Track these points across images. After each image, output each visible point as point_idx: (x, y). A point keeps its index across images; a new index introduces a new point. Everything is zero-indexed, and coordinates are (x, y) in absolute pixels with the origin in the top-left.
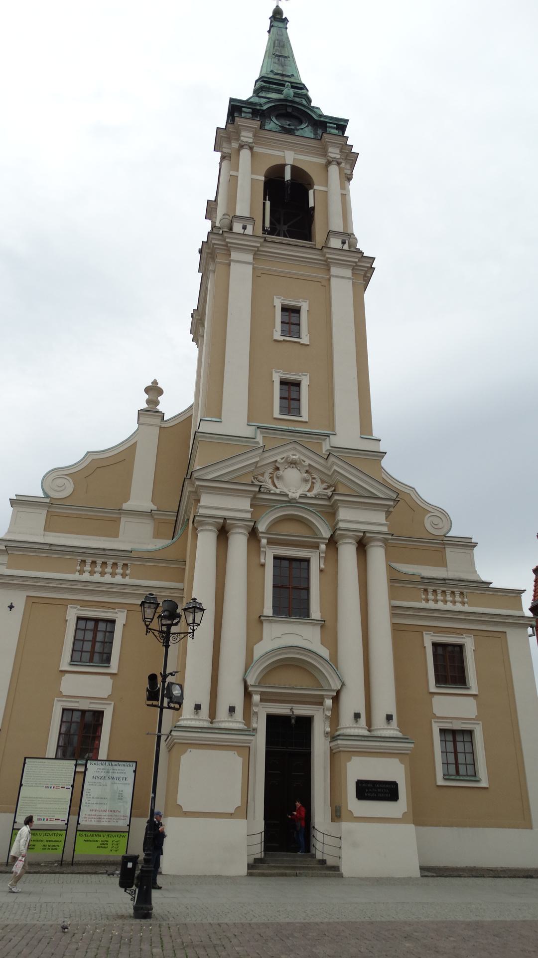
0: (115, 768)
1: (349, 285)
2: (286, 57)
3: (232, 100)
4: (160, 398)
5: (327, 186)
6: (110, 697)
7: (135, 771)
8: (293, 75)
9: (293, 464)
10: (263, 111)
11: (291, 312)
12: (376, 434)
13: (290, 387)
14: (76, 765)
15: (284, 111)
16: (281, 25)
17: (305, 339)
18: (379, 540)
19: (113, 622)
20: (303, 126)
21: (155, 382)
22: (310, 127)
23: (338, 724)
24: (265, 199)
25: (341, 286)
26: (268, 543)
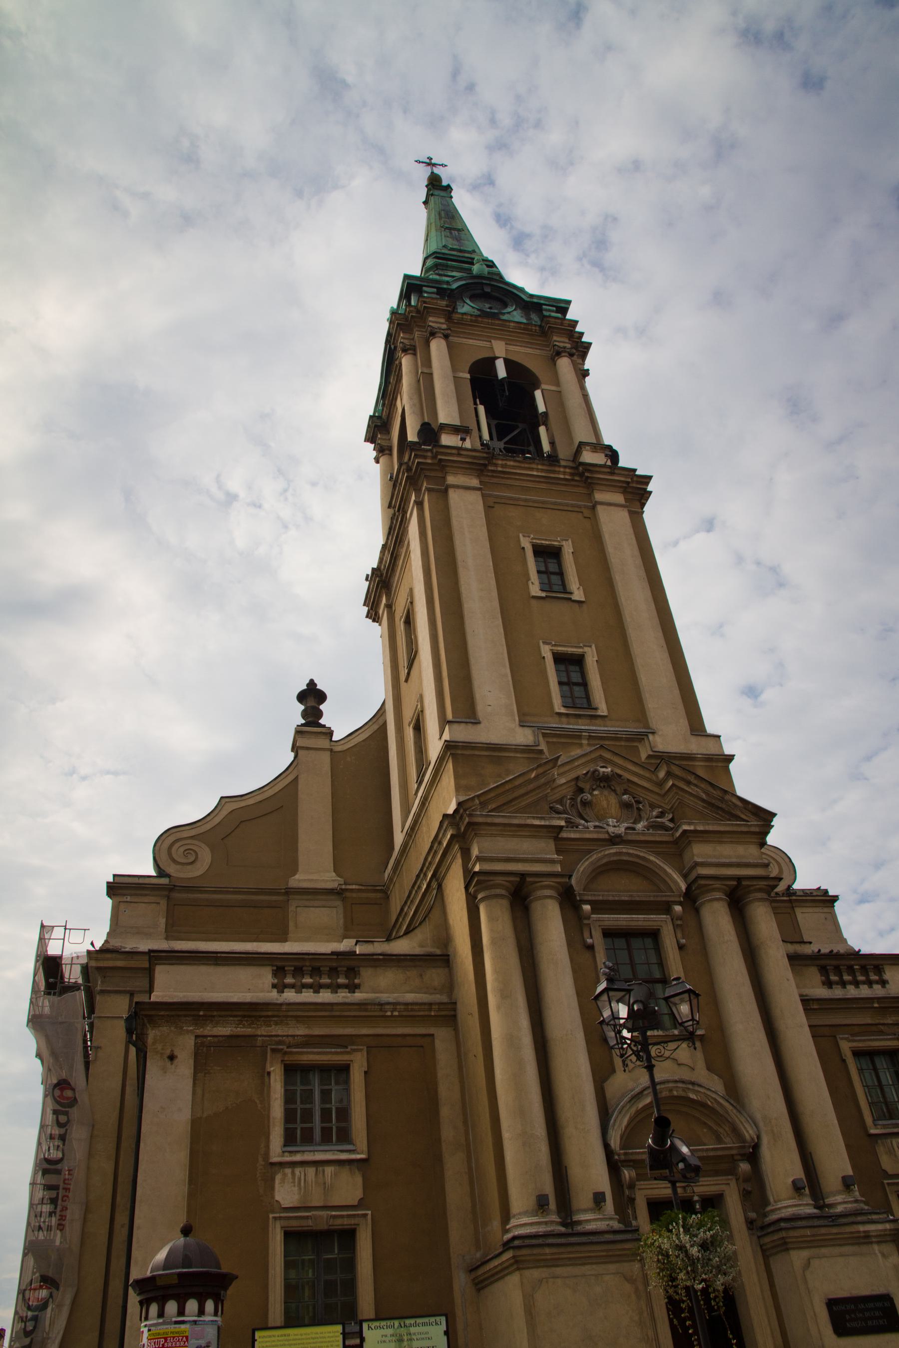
0: (413, 1330)
1: (623, 516)
2: (459, 230)
3: (406, 277)
5: (557, 383)
6: (361, 1204)
7: (446, 1333)
8: (474, 251)
9: (605, 782)
10: (452, 290)
11: (548, 555)
12: (711, 727)
13: (570, 663)
14: (345, 1335)
15: (479, 291)
16: (442, 193)
17: (578, 595)
18: (760, 890)
19: (344, 1069)
20: (509, 309)
21: (312, 684)
22: (519, 311)
23: (765, 1202)
24: (475, 404)
25: (613, 521)
26: (594, 910)
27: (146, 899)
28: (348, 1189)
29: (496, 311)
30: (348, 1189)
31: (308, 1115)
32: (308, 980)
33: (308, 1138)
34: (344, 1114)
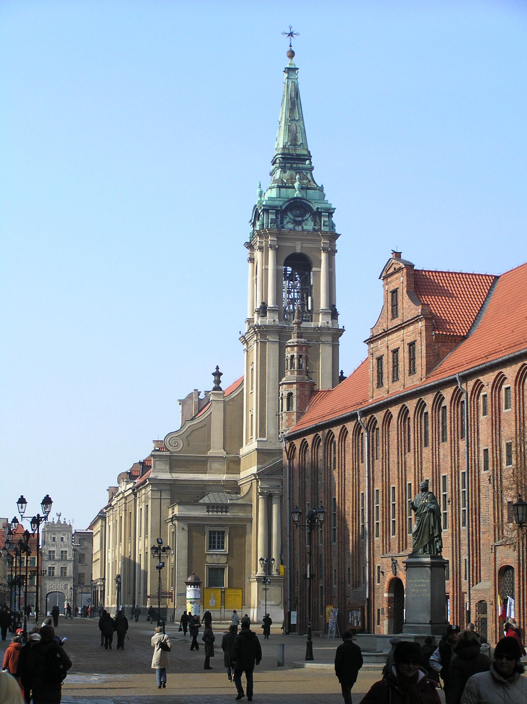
4: (222, 378)
6: (226, 563)
19: (223, 533)
20: (307, 216)
21: (217, 368)
27: (163, 459)
28: (223, 560)
29: (300, 219)
30: (223, 560)
31: (214, 542)
32: (215, 510)
33: (214, 548)
34: (223, 543)
